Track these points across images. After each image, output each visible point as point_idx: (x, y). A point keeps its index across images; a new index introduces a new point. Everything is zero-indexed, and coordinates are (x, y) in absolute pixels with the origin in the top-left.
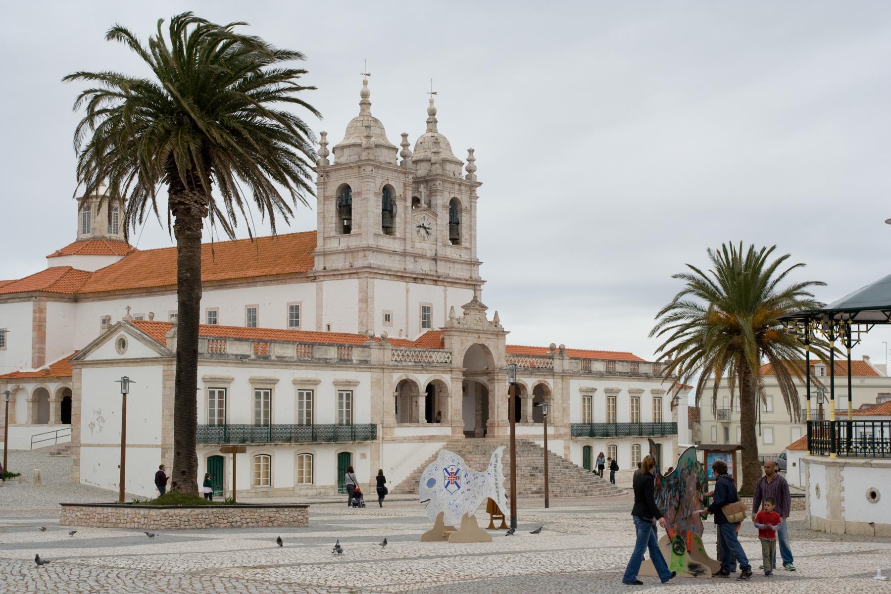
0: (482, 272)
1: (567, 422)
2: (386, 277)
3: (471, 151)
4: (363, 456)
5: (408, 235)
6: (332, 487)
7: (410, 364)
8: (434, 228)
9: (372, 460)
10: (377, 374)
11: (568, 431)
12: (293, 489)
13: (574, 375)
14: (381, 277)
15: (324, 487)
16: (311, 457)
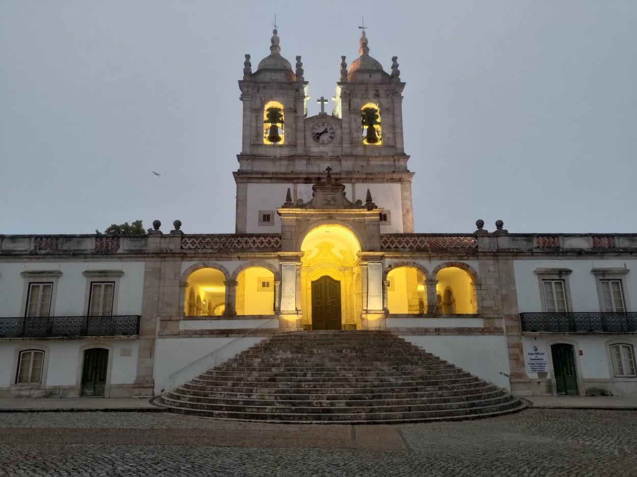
0: (410, 165)
1: (513, 312)
2: (263, 181)
3: (394, 59)
4: (126, 353)
5: (300, 141)
6: (71, 388)
7: (210, 251)
8: (338, 132)
9: (140, 357)
10: (154, 264)
11: (518, 324)
12: (9, 390)
13: (518, 254)
14: (258, 181)
15: (55, 388)
16: (39, 354)
